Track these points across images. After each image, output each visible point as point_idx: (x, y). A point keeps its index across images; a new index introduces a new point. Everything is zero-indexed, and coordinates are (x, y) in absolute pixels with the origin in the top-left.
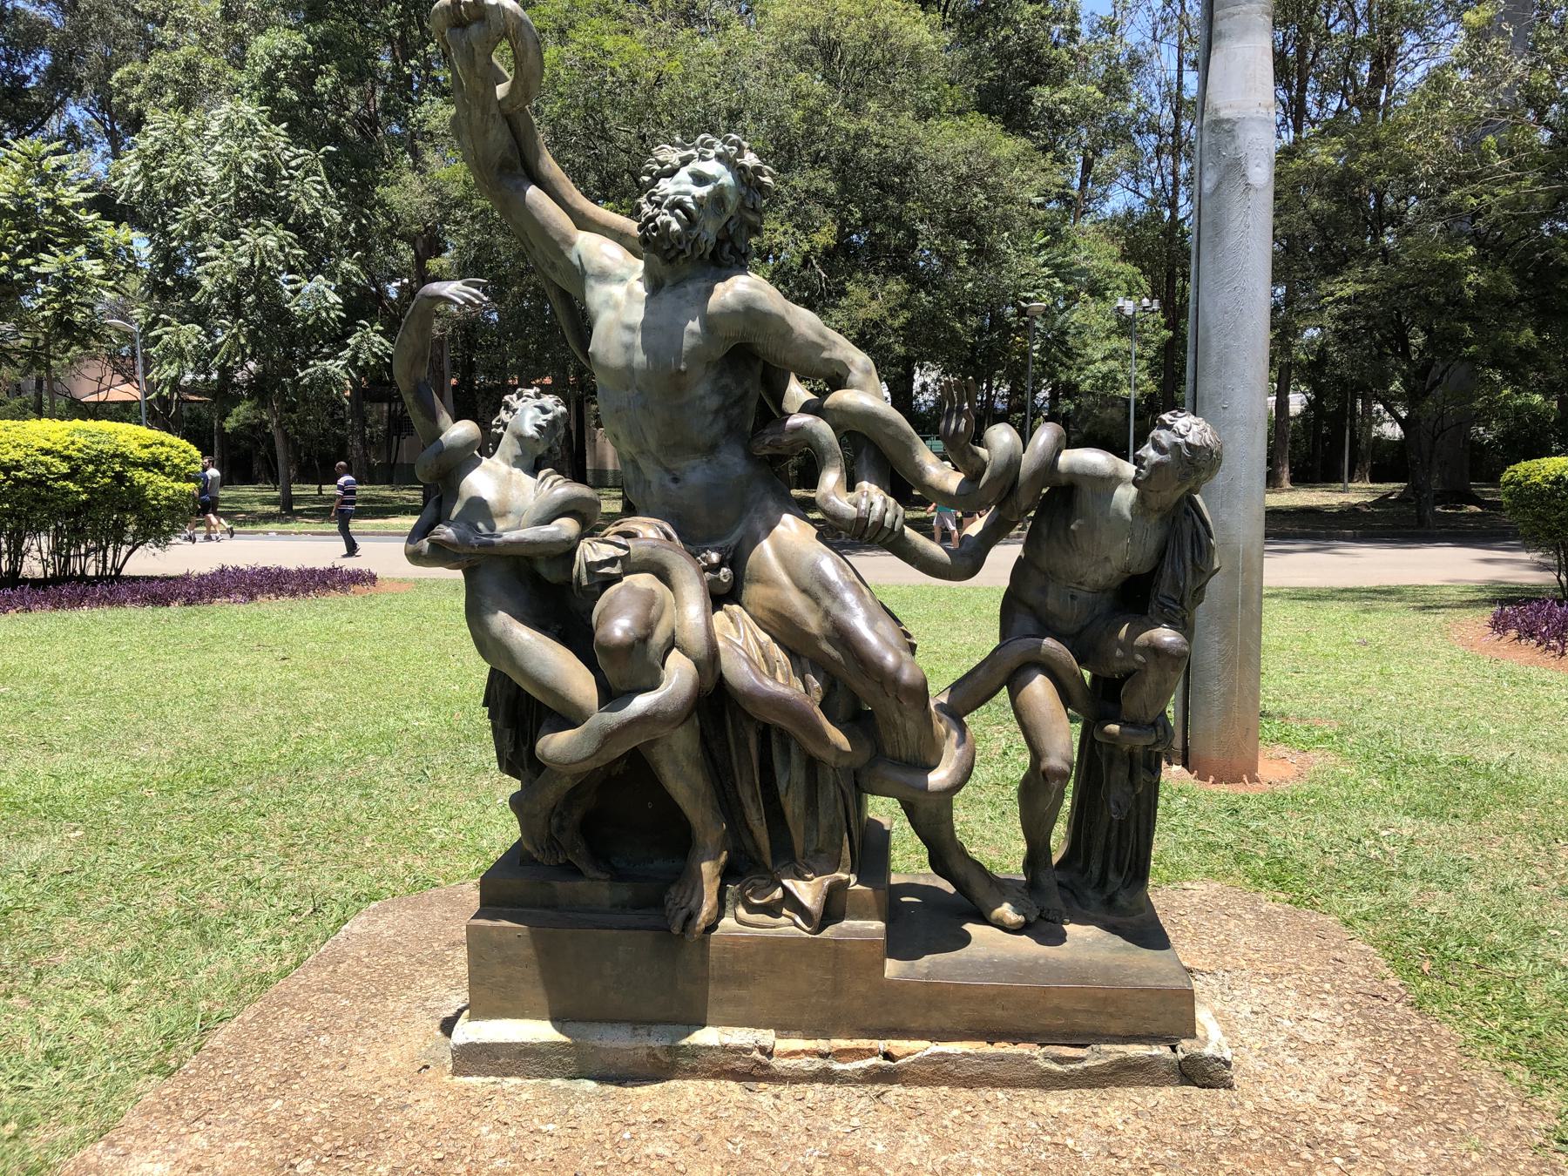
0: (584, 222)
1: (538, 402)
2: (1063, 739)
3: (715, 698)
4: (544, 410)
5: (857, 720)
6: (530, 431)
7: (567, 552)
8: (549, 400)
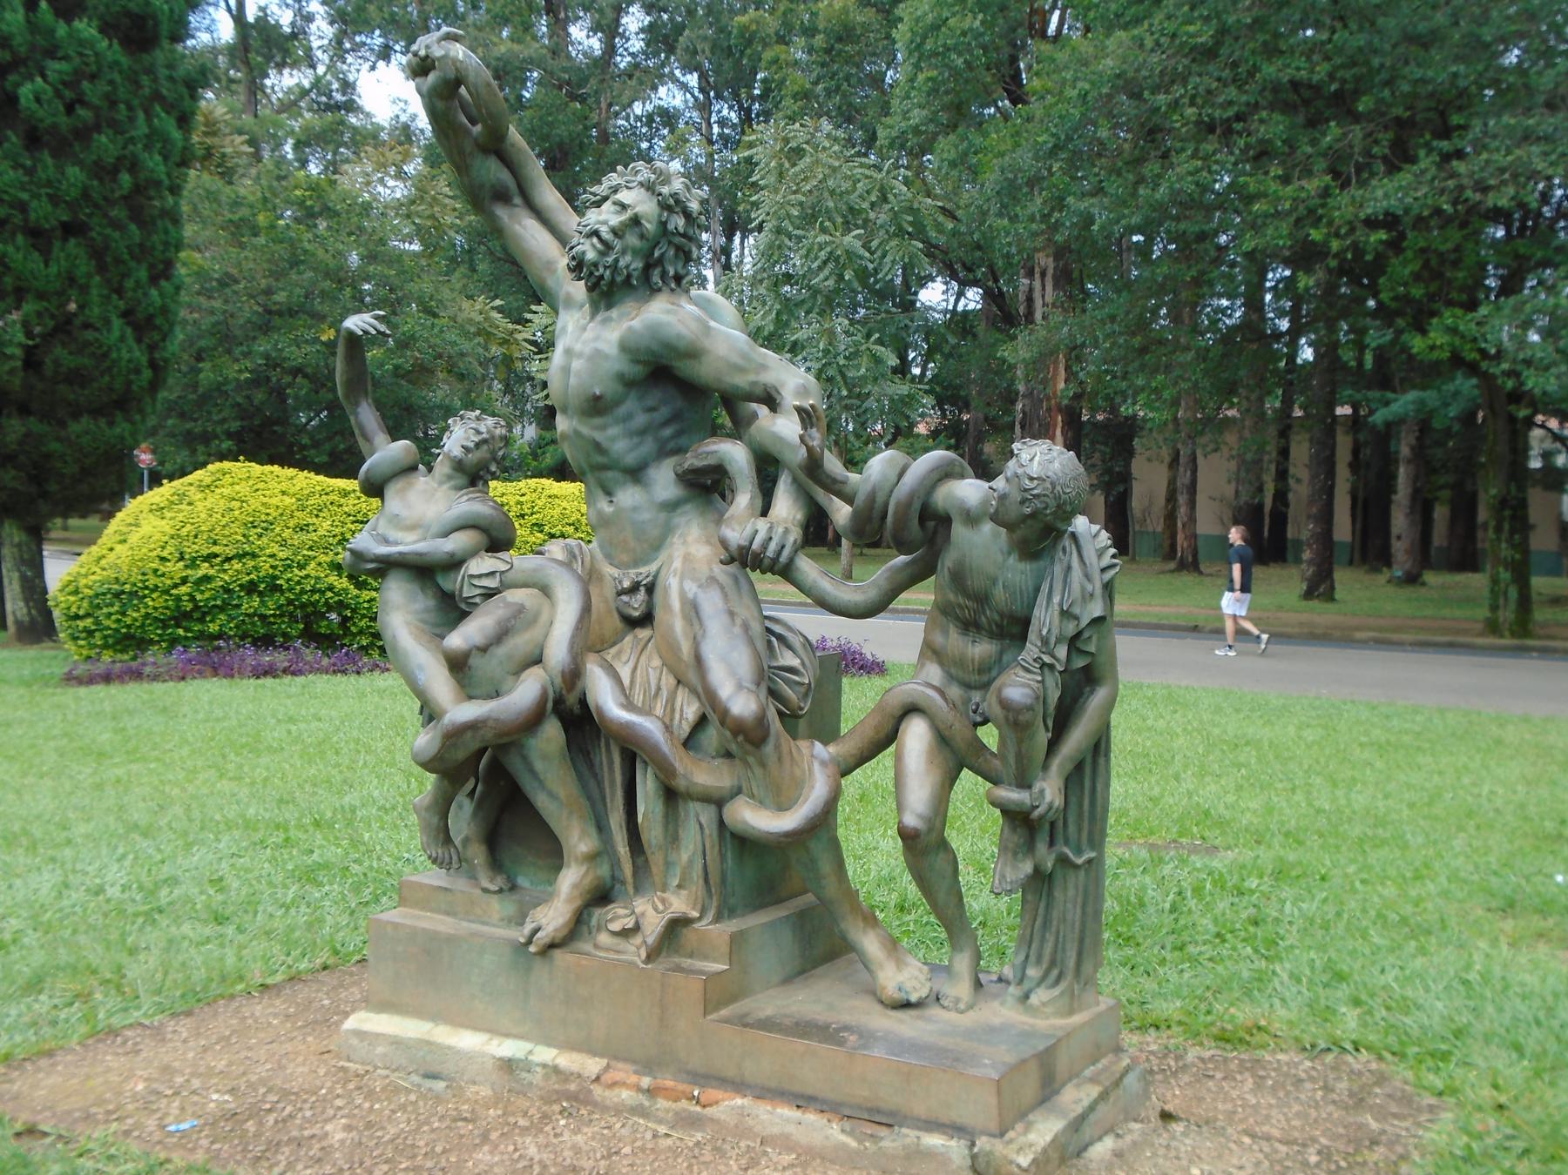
4: (478, 432)
7: (454, 564)
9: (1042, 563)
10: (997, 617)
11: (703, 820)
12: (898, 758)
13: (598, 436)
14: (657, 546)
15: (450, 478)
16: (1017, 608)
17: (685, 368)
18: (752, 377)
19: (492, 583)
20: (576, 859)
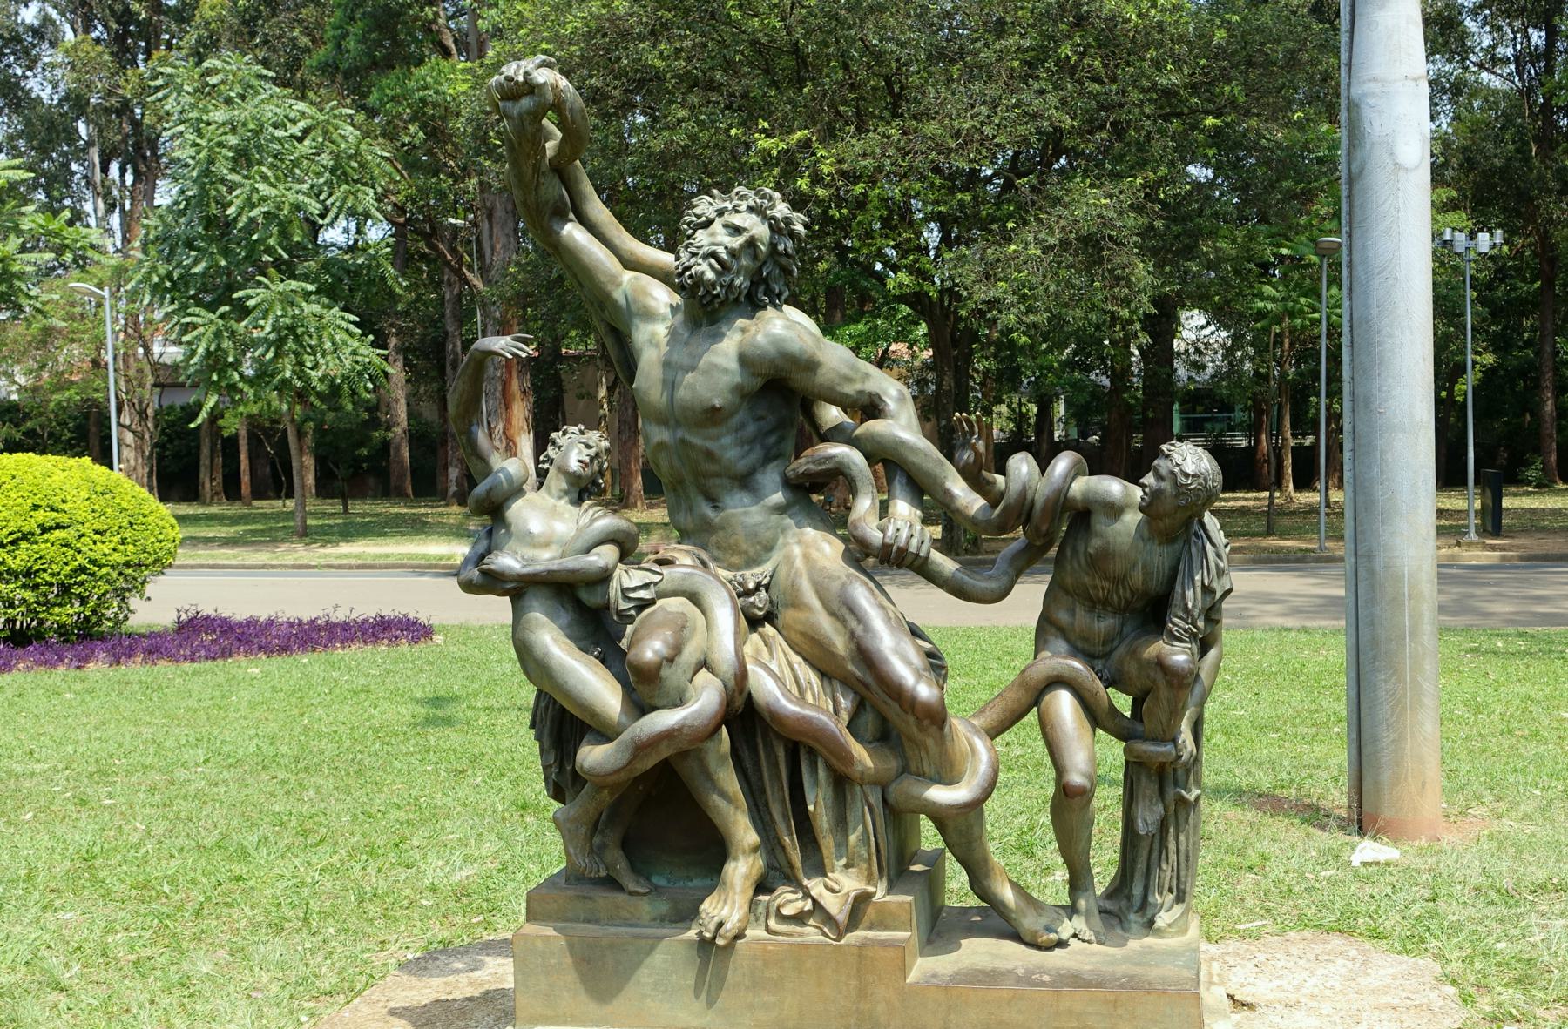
0: (630, 264)
1: (583, 439)
2: (1096, 756)
3: (744, 716)
5: (884, 737)
6: (574, 465)
7: (603, 578)
8: (593, 436)
9: (1178, 546)
10: (1128, 595)
11: (872, 800)
12: (1047, 730)
13: (709, 444)
14: (769, 548)
15: (566, 493)
16: (1155, 585)
17: (799, 380)
18: (858, 386)
19: (642, 594)
20: (744, 852)
